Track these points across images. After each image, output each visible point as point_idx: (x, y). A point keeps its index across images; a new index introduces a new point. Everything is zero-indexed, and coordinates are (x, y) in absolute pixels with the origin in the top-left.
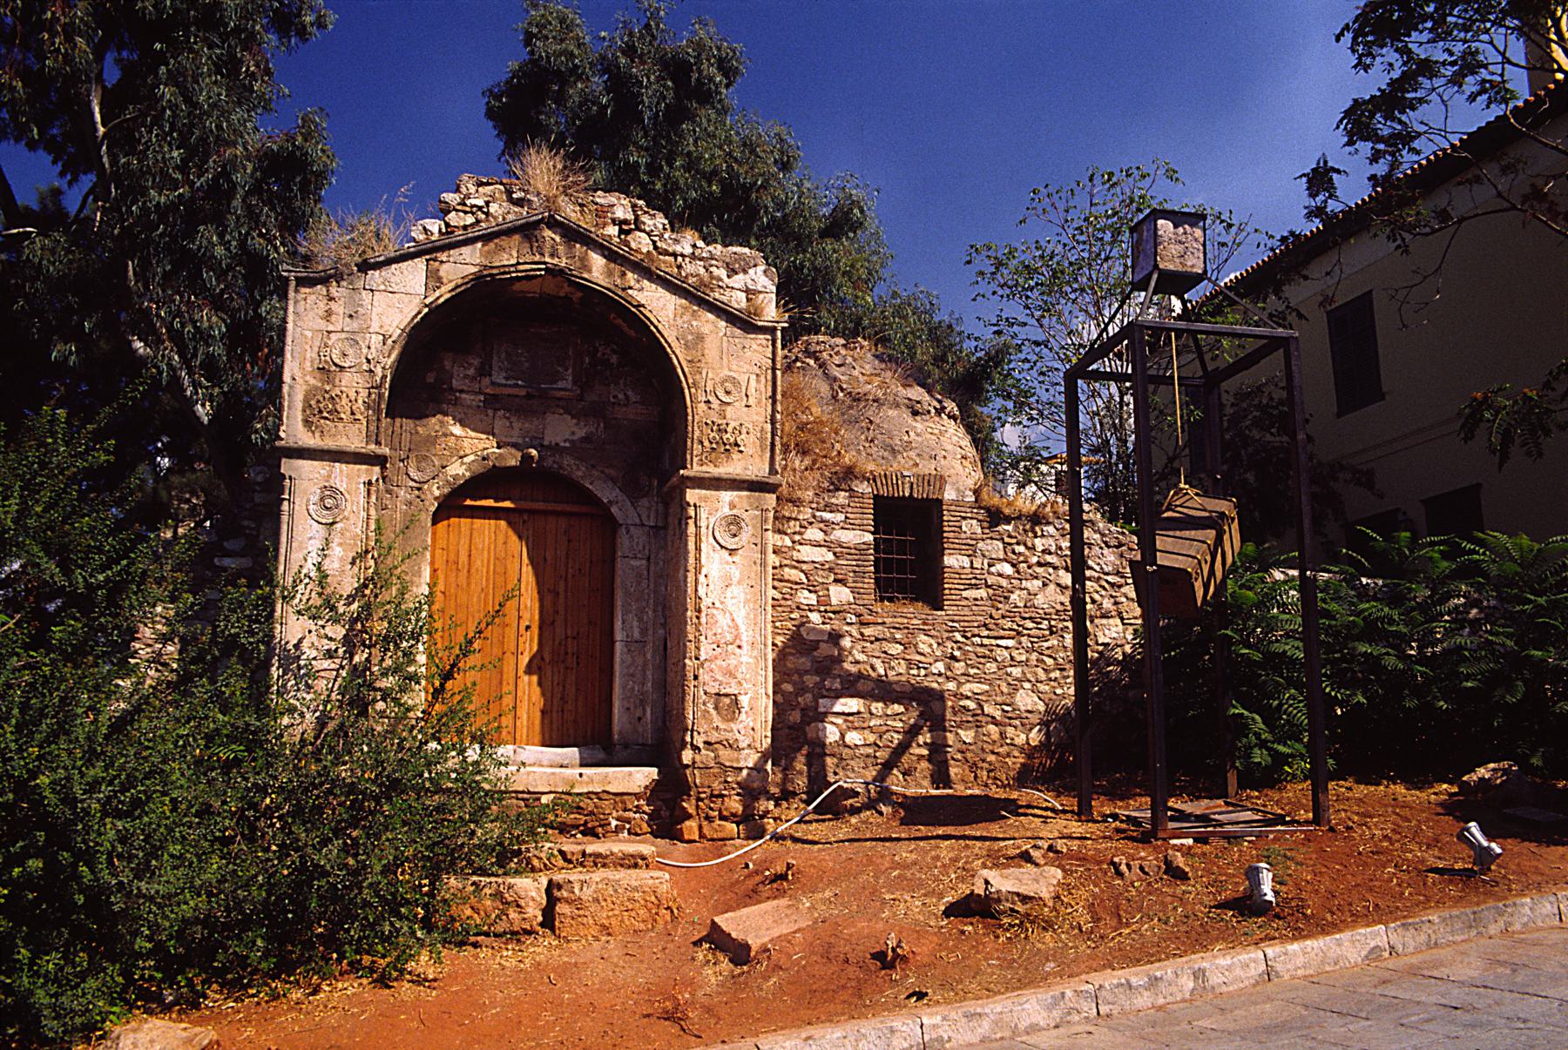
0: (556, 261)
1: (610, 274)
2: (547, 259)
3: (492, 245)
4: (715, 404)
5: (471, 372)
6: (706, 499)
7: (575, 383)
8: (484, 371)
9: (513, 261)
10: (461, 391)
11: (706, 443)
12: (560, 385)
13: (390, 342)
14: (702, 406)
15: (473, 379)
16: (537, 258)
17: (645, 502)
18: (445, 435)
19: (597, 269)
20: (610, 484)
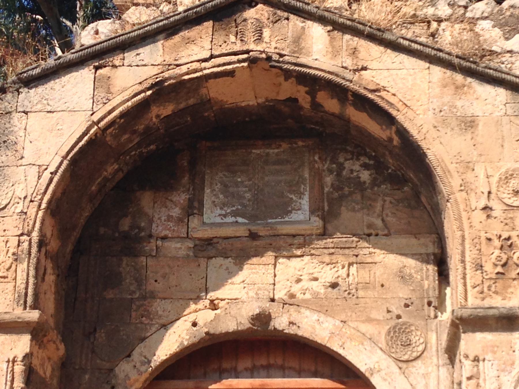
0: (259, 48)
1: (335, 53)
2: (252, 46)
3: (177, 38)
4: (498, 209)
5: (176, 212)
6: (493, 348)
7: (312, 212)
8: (194, 208)
9: (207, 54)
10: (164, 238)
11: (488, 267)
12: (295, 216)
13: (47, 175)
14: (479, 216)
15: (180, 220)
16: (238, 47)
17: (419, 366)
18: (144, 298)
19: (319, 50)
20: (367, 343)
